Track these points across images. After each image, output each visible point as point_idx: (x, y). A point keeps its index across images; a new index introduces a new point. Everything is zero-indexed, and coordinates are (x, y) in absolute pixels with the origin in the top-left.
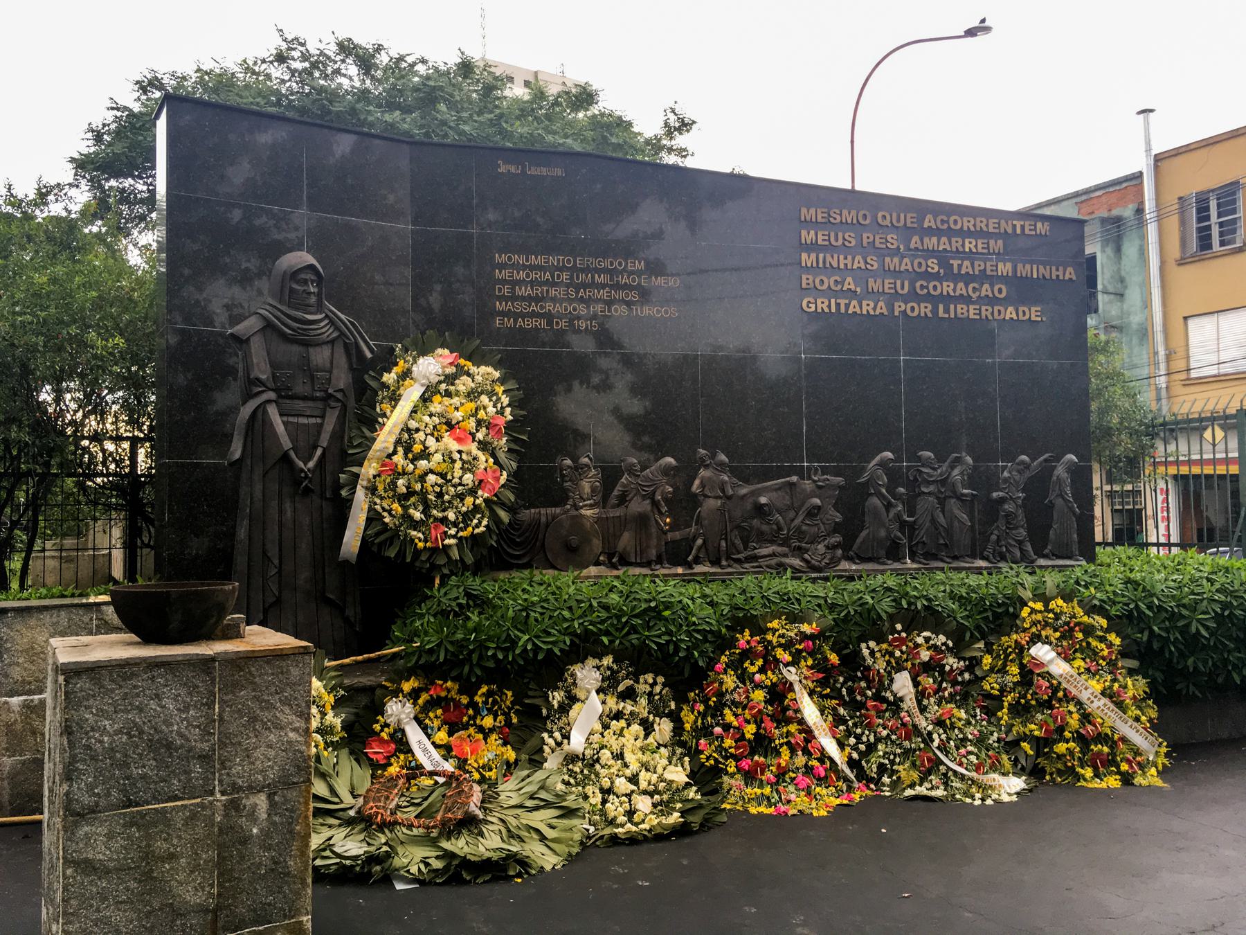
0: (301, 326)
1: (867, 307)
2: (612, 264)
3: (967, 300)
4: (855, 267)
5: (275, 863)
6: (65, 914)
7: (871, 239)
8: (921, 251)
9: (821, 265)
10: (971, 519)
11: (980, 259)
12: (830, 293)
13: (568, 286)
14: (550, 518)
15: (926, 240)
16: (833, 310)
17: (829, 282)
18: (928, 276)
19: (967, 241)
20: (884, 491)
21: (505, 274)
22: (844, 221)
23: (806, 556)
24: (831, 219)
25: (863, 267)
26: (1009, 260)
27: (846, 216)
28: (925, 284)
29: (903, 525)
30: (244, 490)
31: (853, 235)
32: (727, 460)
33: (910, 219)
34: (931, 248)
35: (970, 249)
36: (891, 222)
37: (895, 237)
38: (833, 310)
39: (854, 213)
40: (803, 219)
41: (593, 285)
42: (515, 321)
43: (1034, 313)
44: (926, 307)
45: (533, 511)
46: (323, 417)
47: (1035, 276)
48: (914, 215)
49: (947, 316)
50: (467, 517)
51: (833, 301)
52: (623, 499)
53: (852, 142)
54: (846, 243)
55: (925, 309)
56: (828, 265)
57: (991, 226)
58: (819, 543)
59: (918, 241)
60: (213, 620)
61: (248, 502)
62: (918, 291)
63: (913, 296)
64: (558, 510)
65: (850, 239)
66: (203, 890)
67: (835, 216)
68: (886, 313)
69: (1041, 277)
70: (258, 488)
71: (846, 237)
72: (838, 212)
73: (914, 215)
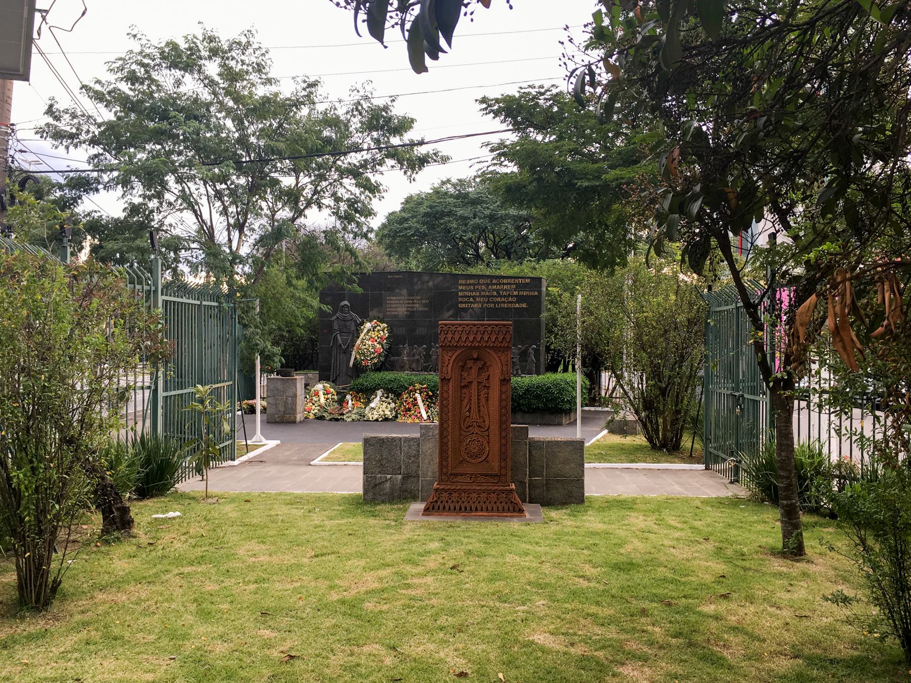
3: (504, 302)
12: (466, 302)
18: (493, 296)
33: (489, 281)
43: (524, 305)
50: (373, 358)
52: (414, 355)
55: (492, 305)
63: (488, 302)
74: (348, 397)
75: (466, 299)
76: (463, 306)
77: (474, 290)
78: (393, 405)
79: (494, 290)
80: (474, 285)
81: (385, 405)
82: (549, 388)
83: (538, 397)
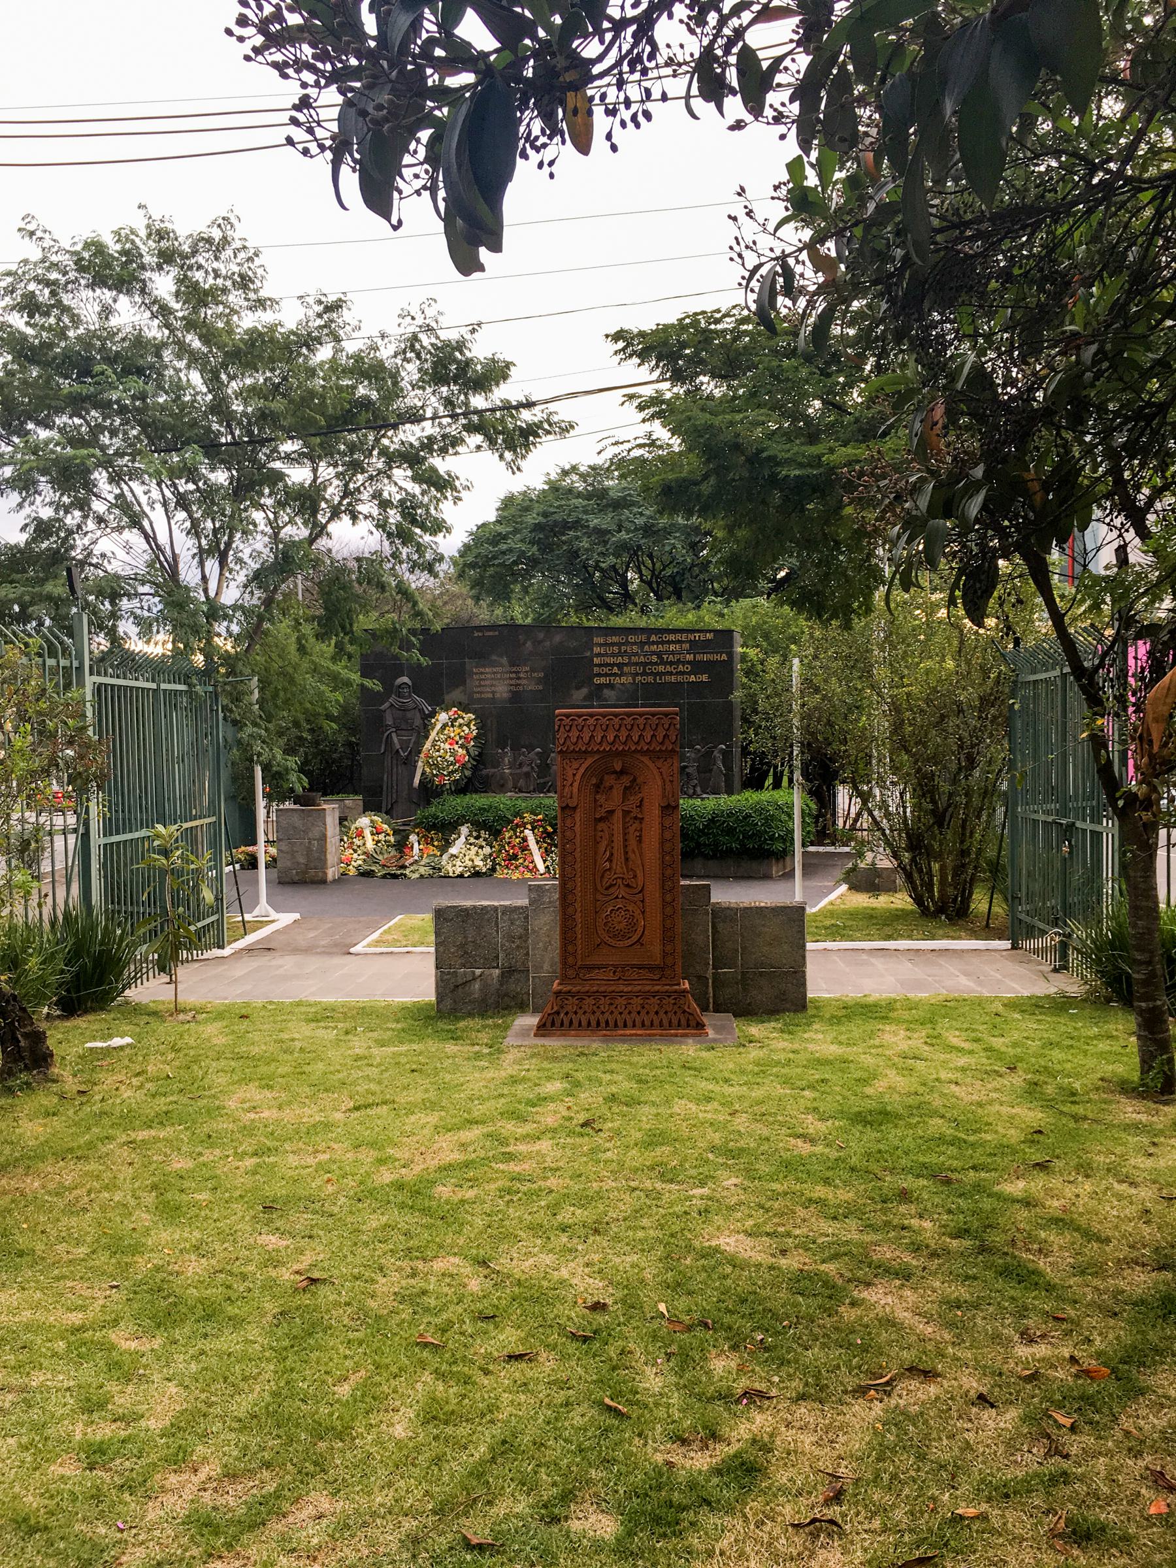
3: (671, 674)
12: (606, 675)
18: (651, 663)
27: (615, 639)
33: (644, 638)
50: (453, 772)
52: (521, 765)
55: (650, 679)
63: (644, 673)
74: (413, 838)
75: (606, 670)
76: (602, 680)
77: (620, 654)
78: (487, 850)
79: (654, 653)
80: (619, 644)
81: (474, 849)
82: (748, 816)
83: (730, 831)
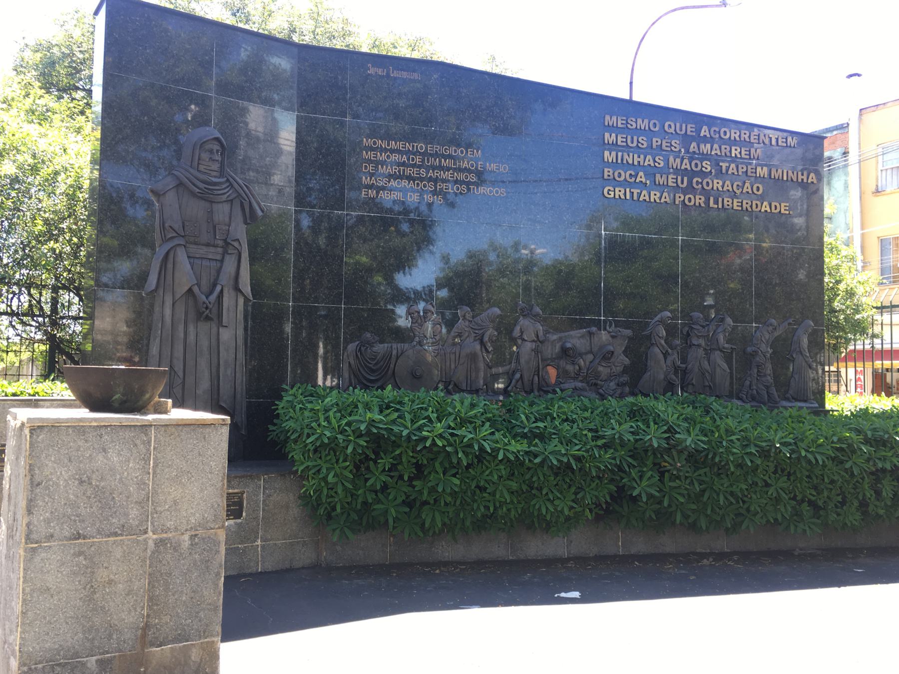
0: (207, 186)
1: (655, 196)
2: (455, 152)
4: (646, 164)
5: (194, 592)
6: (23, 624)
7: (659, 143)
8: (698, 154)
9: (619, 161)
10: (730, 368)
11: (741, 163)
12: (625, 184)
13: (420, 167)
14: (400, 352)
15: (702, 146)
16: (628, 197)
17: (625, 175)
18: (703, 174)
19: (733, 148)
20: (663, 342)
21: (371, 155)
22: (638, 127)
23: (601, 391)
24: (629, 126)
25: (652, 165)
26: (766, 165)
27: (642, 124)
28: (700, 180)
29: (676, 369)
30: (157, 315)
31: (645, 139)
32: (541, 312)
33: (690, 129)
34: (705, 152)
35: (736, 154)
36: (675, 130)
37: (678, 142)
38: (628, 197)
39: (646, 121)
40: (606, 124)
41: (441, 168)
42: (378, 193)
44: (700, 199)
45: (386, 345)
46: (222, 261)
47: (785, 178)
48: (694, 126)
49: (716, 206)
51: (628, 190)
53: (631, 83)
54: (639, 145)
56: (625, 162)
57: (752, 138)
58: (612, 381)
59: (696, 146)
60: (147, 396)
61: (160, 325)
62: (695, 185)
64: (406, 345)
65: (642, 142)
66: (136, 611)
67: (631, 123)
68: (669, 202)
69: (789, 179)
70: (168, 312)
71: (640, 140)
72: (634, 120)
73: (694, 126)
76: (619, 192)
